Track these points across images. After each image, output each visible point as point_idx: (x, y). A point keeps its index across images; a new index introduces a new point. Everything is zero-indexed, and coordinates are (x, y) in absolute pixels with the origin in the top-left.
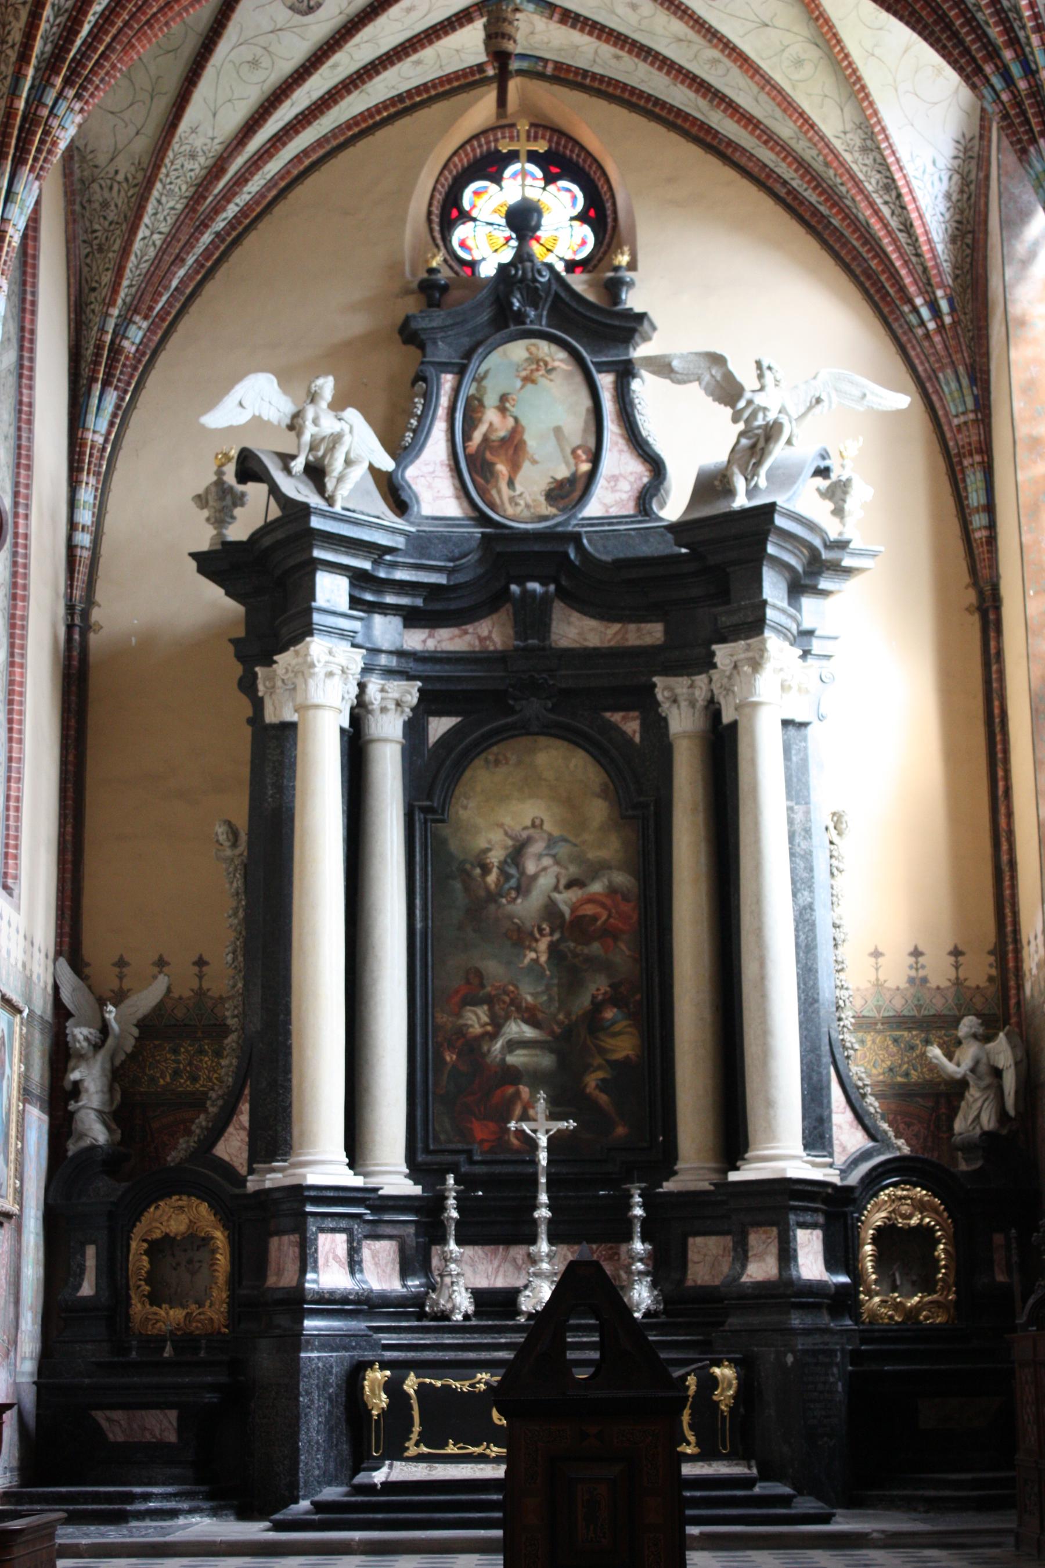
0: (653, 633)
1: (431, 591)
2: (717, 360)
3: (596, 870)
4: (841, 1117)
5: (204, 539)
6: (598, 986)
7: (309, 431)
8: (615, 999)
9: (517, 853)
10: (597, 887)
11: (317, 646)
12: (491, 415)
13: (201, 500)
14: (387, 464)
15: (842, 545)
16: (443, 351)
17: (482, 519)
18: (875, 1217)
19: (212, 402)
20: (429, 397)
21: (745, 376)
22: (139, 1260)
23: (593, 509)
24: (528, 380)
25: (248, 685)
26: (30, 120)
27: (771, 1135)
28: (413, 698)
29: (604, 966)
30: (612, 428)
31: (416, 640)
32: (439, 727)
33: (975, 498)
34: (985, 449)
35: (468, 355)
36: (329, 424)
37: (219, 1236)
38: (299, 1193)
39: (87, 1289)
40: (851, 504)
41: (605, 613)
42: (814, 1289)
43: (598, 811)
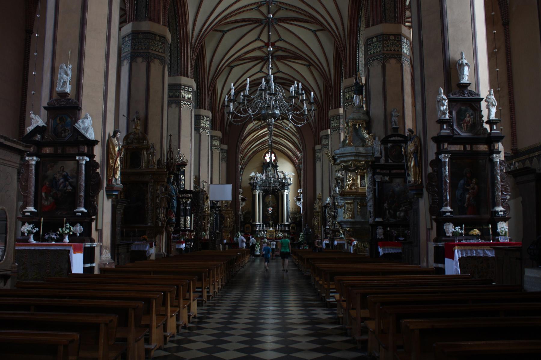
2: (282, 171)
4: (289, 220)
5: (249, 182)
7: (256, 176)
9: (269, 202)
13: (249, 179)
15: (290, 183)
19: (250, 175)
21: (284, 172)
22: (245, 228)
25: (252, 191)
26: (241, 162)
27: (284, 221)
28: (262, 192)
32: (264, 193)
33: (300, 178)
34: (301, 175)
36: (258, 176)
37: (250, 227)
38: (256, 224)
39: (242, 230)
40: (291, 180)
42: (287, 230)
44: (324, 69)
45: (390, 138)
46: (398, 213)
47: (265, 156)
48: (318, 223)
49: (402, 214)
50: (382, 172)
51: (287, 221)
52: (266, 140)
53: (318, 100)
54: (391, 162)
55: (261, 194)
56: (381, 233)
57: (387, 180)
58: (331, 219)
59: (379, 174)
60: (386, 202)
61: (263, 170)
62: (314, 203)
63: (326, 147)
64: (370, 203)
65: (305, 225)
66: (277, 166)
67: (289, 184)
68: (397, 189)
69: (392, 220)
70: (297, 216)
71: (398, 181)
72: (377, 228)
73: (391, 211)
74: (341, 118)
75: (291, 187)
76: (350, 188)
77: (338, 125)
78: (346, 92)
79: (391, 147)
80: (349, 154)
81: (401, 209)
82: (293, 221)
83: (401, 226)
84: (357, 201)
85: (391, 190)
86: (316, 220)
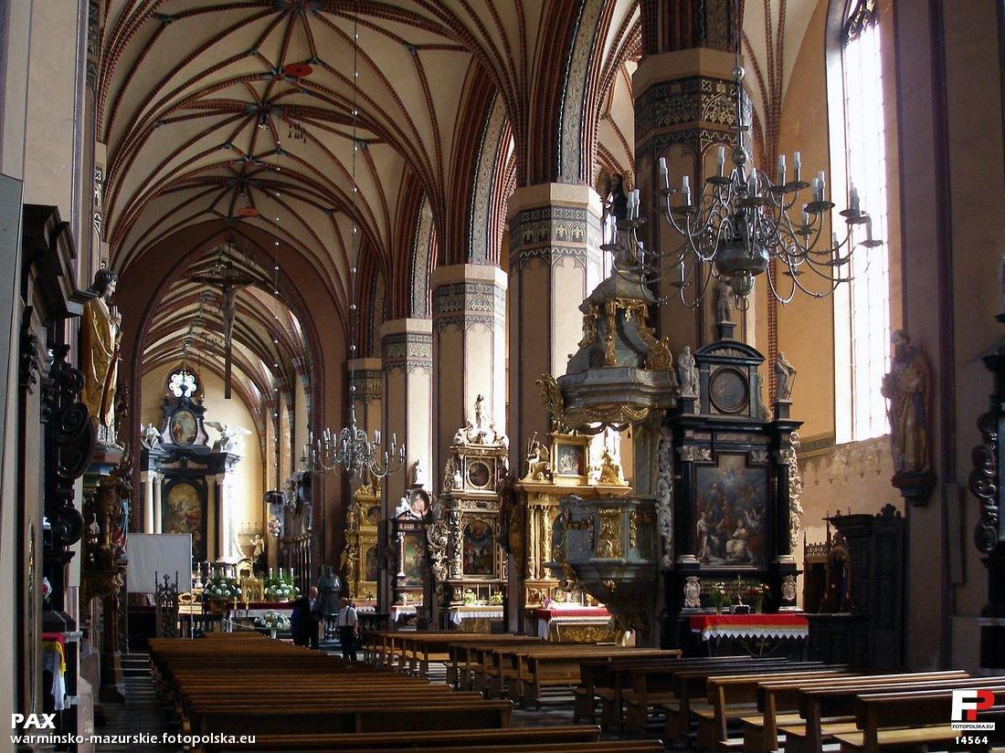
0: (205, 466)
1: (167, 458)
3: (194, 507)
6: (194, 528)
8: (197, 529)
10: (194, 510)
11: (149, 472)
12: (178, 425)
14: (159, 435)
16: (168, 412)
17: (175, 444)
18: (239, 568)
20: (166, 421)
23: (195, 443)
24: (184, 418)
27: (223, 555)
29: (195, 524)
30: (199, 428)
31: (163, 466)
32: (167, 481)
33: (263, 444)
34: (265, 435)
35: (173, 413)
41: (197, 463)
43: (195, 497)
44: (425, 154)
45: (715, 350)
46: (729, 544)
47: (169, 381)
48: (357, 563)
49: (740, 546)
50: (699, 436)
51: (231, 555)
52: (181, 336)
53: (380, 237)
54: (717, 412)
55: (159, 482)
56: (696, 595)
57: (705, 460)
58: (439, 554)
59: (691, 441)
60: (703, 515)
61: (165, 417)
62: (347, 511)
63: (399, 366)
64: (666, 516)
65: (320, 568)
66: (204, 410)
67: (235, 459)
68: (729, 482)
69: (717, 564)
70: (254, 544)
71: (731, 462)
72: (686, 582)
73: (713, 538)
74: (468, 290)
75: (238, 466)
76: (535, 477)
77: (459, 309)
78: (526, 222)
79: (718, 373)
80: (616, 388)
81: (736, 534)
82: (245, 557)
83: (739, 577)
84: (630, 510)
85: (715, 485)
86: (351, 556)
